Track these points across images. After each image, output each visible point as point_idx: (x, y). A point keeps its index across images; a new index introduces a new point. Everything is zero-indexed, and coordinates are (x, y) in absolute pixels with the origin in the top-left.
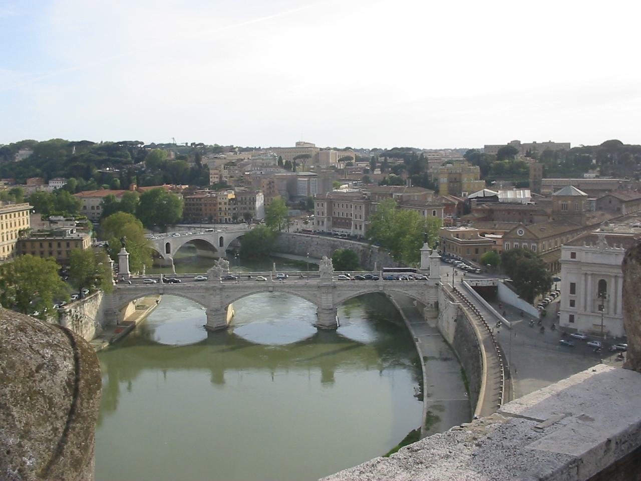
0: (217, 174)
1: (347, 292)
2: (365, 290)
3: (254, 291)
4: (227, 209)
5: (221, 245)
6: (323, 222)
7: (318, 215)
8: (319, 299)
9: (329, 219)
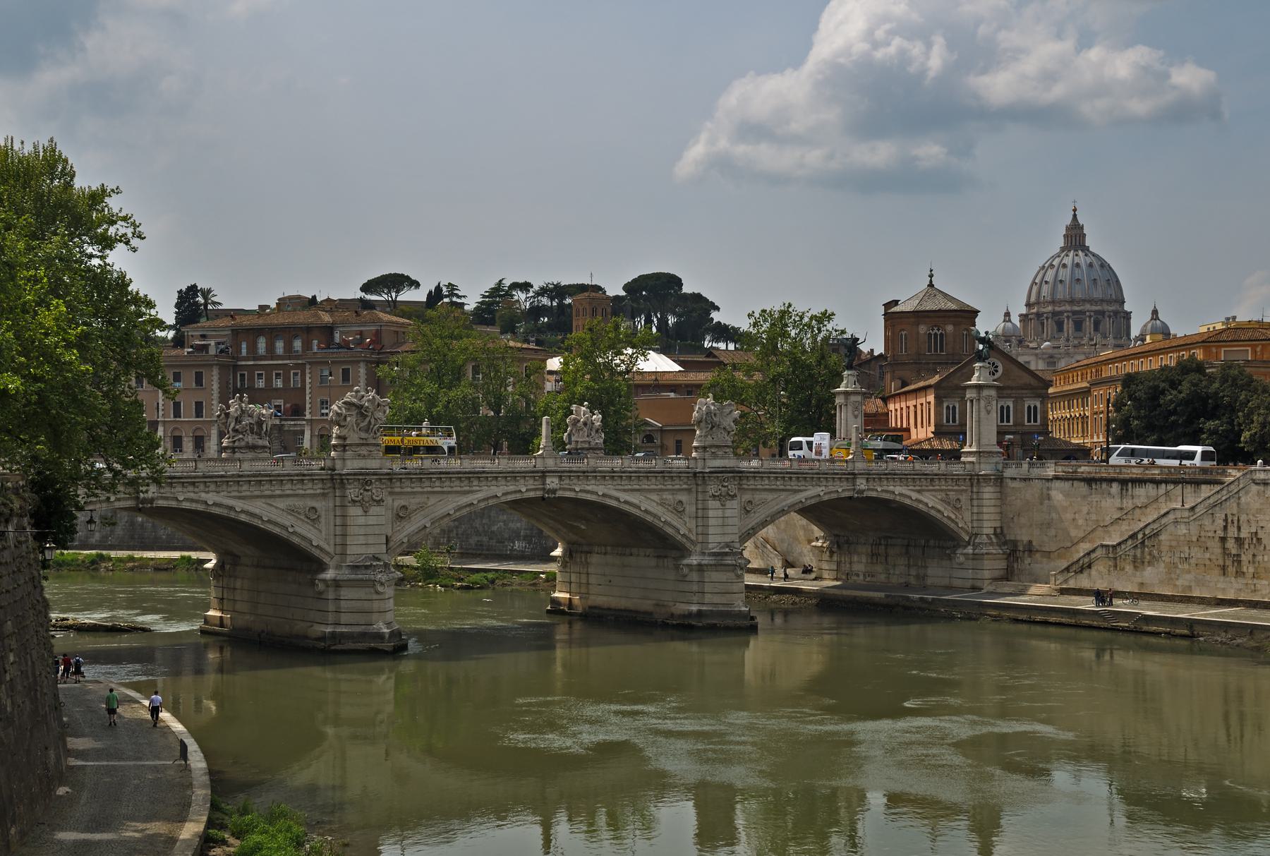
1: (770, 496)
2: (819, 490)
8: (692, 524)
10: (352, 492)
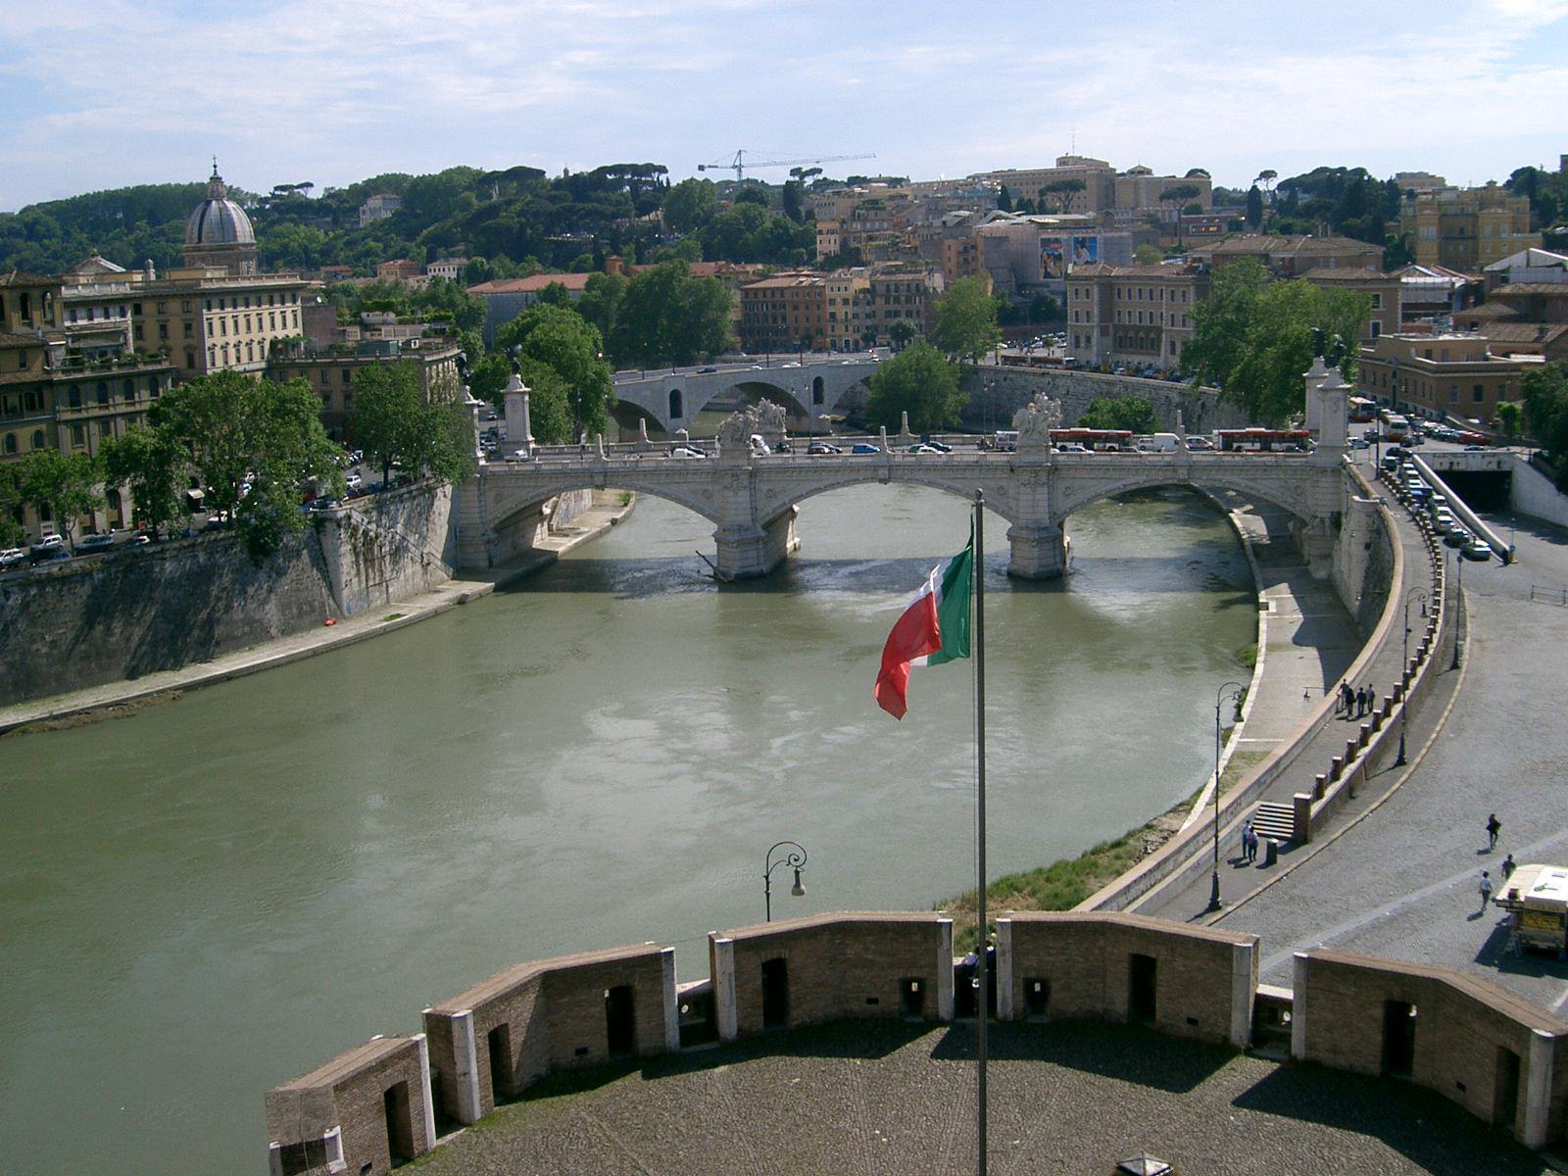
0: (833, 233)
3: (839, 478)
4: (850, 316)
5: (818, 398)
6: (1088, 340)
7: (1077, 321)
9: (1104, 332)
10: (728, 480)
